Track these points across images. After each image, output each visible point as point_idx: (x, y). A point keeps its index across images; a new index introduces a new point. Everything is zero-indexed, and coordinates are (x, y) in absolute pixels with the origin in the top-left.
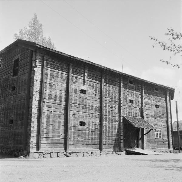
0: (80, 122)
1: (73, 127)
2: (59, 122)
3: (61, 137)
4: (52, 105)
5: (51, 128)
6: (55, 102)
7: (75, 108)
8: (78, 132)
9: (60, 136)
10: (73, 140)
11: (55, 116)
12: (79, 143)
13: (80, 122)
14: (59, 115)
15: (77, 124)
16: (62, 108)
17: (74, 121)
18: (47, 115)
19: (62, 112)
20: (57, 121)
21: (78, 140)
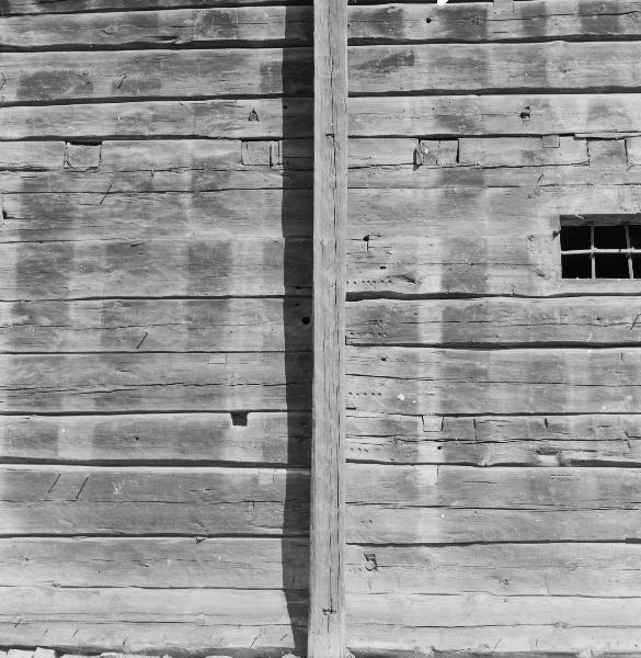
0: (573, 233)
1: (430, 311)
2: (209, 262)
3: (239, 444)
4: (101, 69)
5: (80, 336)
6: (143, 24)
7: (459, 52)
8: (541, 375)
9: (215, 436)
10: (447, 483)
11: (148, 189)
12: (569, 524)
13: (573, 233)
14: (199, 168)
15: (521, 262)
16: (254, 83)
17: (461, 227)
18: (27, 191)
19: (257, 130)
20: (165, 253)
21: (535, 486)
